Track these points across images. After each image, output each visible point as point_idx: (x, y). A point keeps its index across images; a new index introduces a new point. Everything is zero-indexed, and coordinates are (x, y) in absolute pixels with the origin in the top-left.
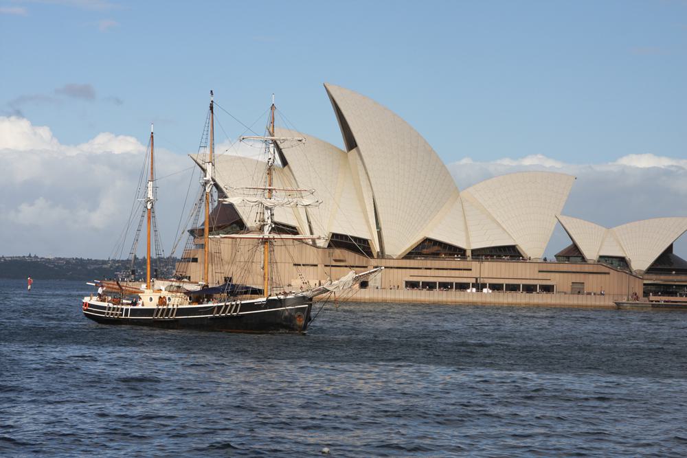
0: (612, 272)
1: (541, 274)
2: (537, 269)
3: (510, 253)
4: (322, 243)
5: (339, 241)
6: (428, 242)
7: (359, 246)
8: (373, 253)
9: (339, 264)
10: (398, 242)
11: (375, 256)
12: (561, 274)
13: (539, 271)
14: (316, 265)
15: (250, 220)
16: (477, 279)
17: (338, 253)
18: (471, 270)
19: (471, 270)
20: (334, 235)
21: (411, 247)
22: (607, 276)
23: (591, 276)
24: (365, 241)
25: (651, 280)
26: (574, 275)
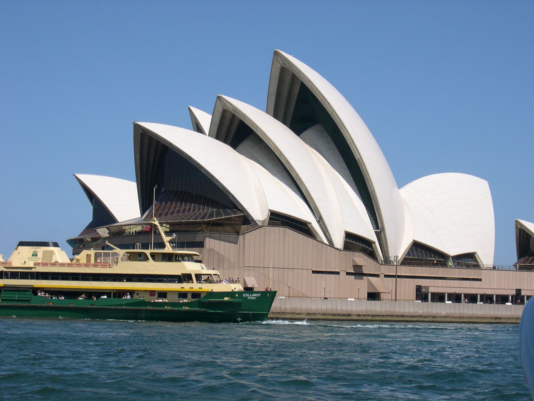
4: (339, 241)
5: (353, 241)
11: (380, 262)
16: (519, 291)
17: (361, 259)
18: (480, 280)
19: (480, 280)
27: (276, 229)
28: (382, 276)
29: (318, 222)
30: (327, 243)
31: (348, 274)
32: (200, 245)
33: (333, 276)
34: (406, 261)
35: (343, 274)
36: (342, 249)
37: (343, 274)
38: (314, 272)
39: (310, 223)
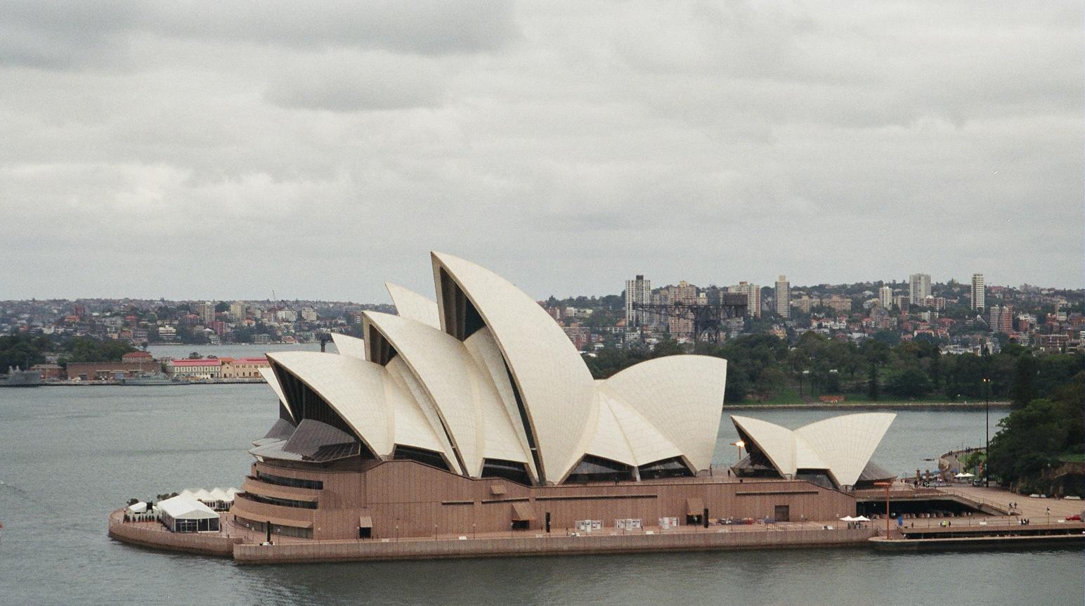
3: (676, 469)
4: (475, 470)
5: (494, 469)
6: (588, 459)
7: (513, 472)
8: (532, 480)
11: (533, 482)
15: (382, 449)
20: (487, 461)
22: (815, 495)
24: (521, 465)
26: (777, 497)
27: (400, 464)
28: (532, 501)
29: (454, 450)
30: (460, 472)
32: (319, 486)
33: (465, 507)
34: (572, 478)
35: (478, 505)
36: (482, 476)
37: (478, 505)
38: (444, 504)
39: (443, 454)
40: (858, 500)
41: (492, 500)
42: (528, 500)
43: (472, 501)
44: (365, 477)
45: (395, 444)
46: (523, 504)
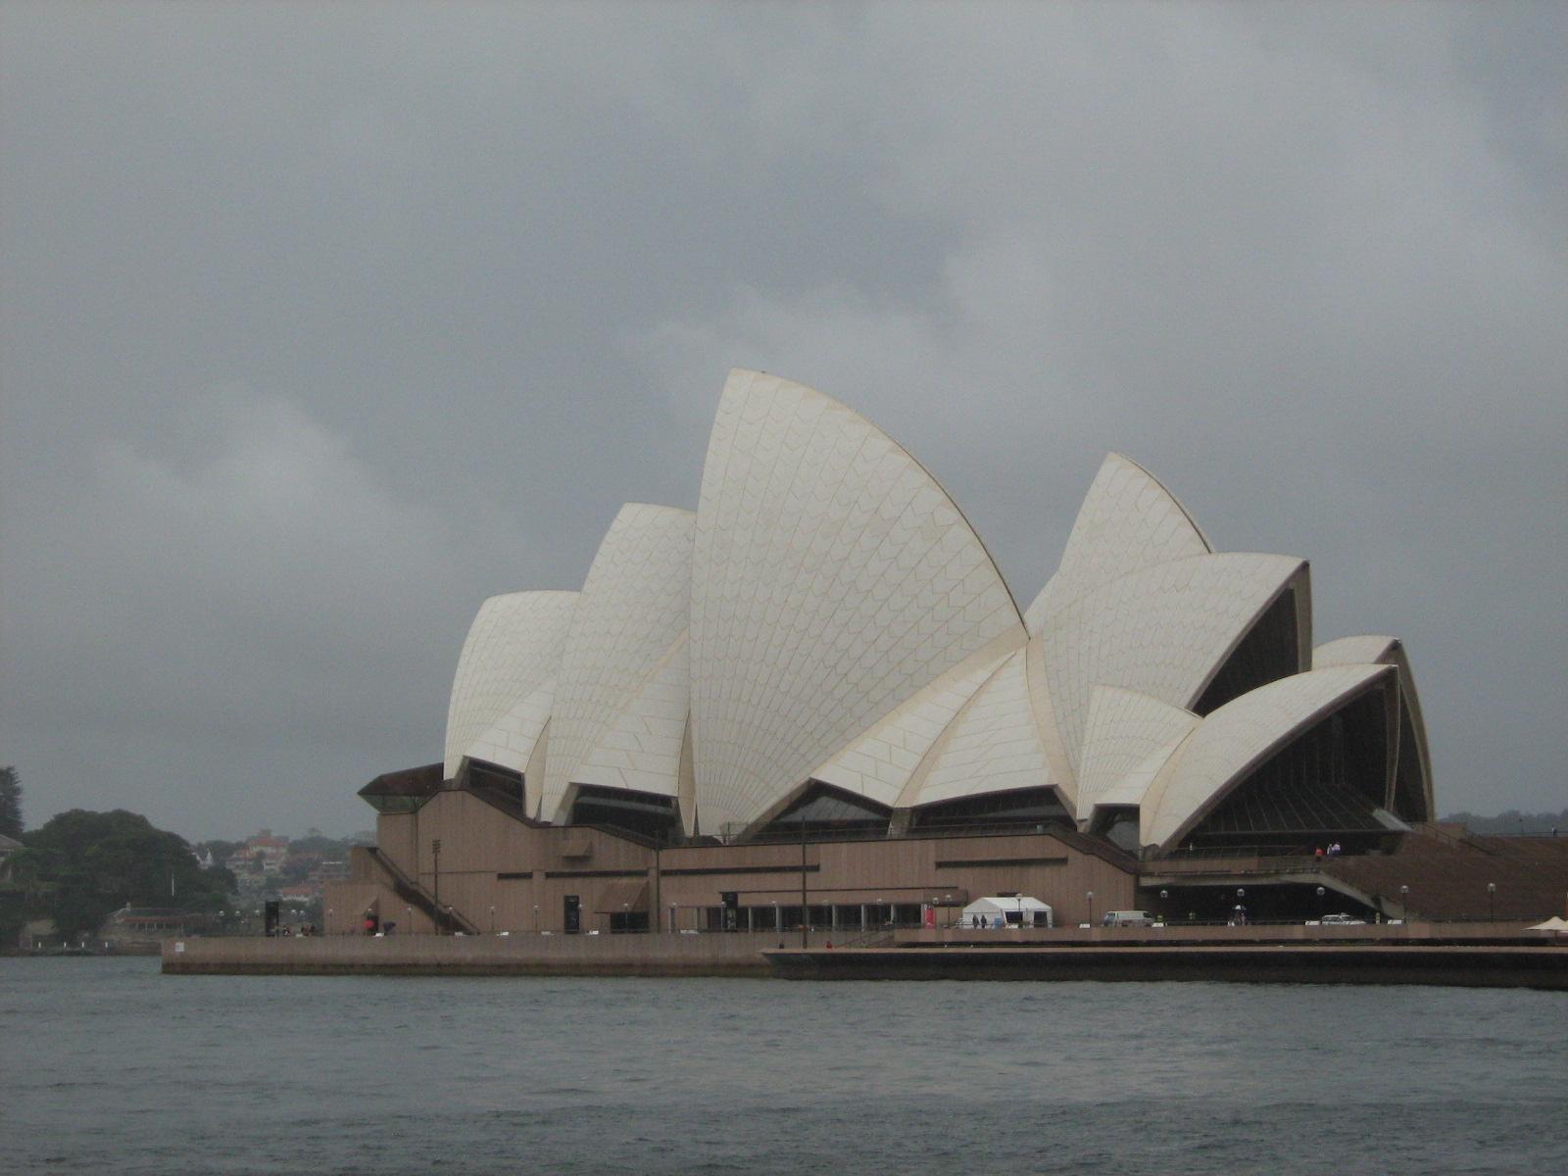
0: (1073, 855)
1: (940, 871)
2: (932, 859)
9: (577, 867)
10: (731, 798)
12: (977, 871)
13: (940, 865)
14: (528, 876)
17: (577, 842)
20: (586, 790)
21: (773, 809)
22: (1063, 869)
23: (1032, 871)
24: (665, 801)
25: (1151, 875)
30: (531, 812)
31: (548, 875)
35: (536, 876)
36: (562, 821)
37: (538, 878)
38: (501, 876)
40: (1146, 882)
41: (566, 870)
42: (643, 874)
43: (528, 870)
44: (417, 819)
45: (465, 757)
46: (634, 881)
